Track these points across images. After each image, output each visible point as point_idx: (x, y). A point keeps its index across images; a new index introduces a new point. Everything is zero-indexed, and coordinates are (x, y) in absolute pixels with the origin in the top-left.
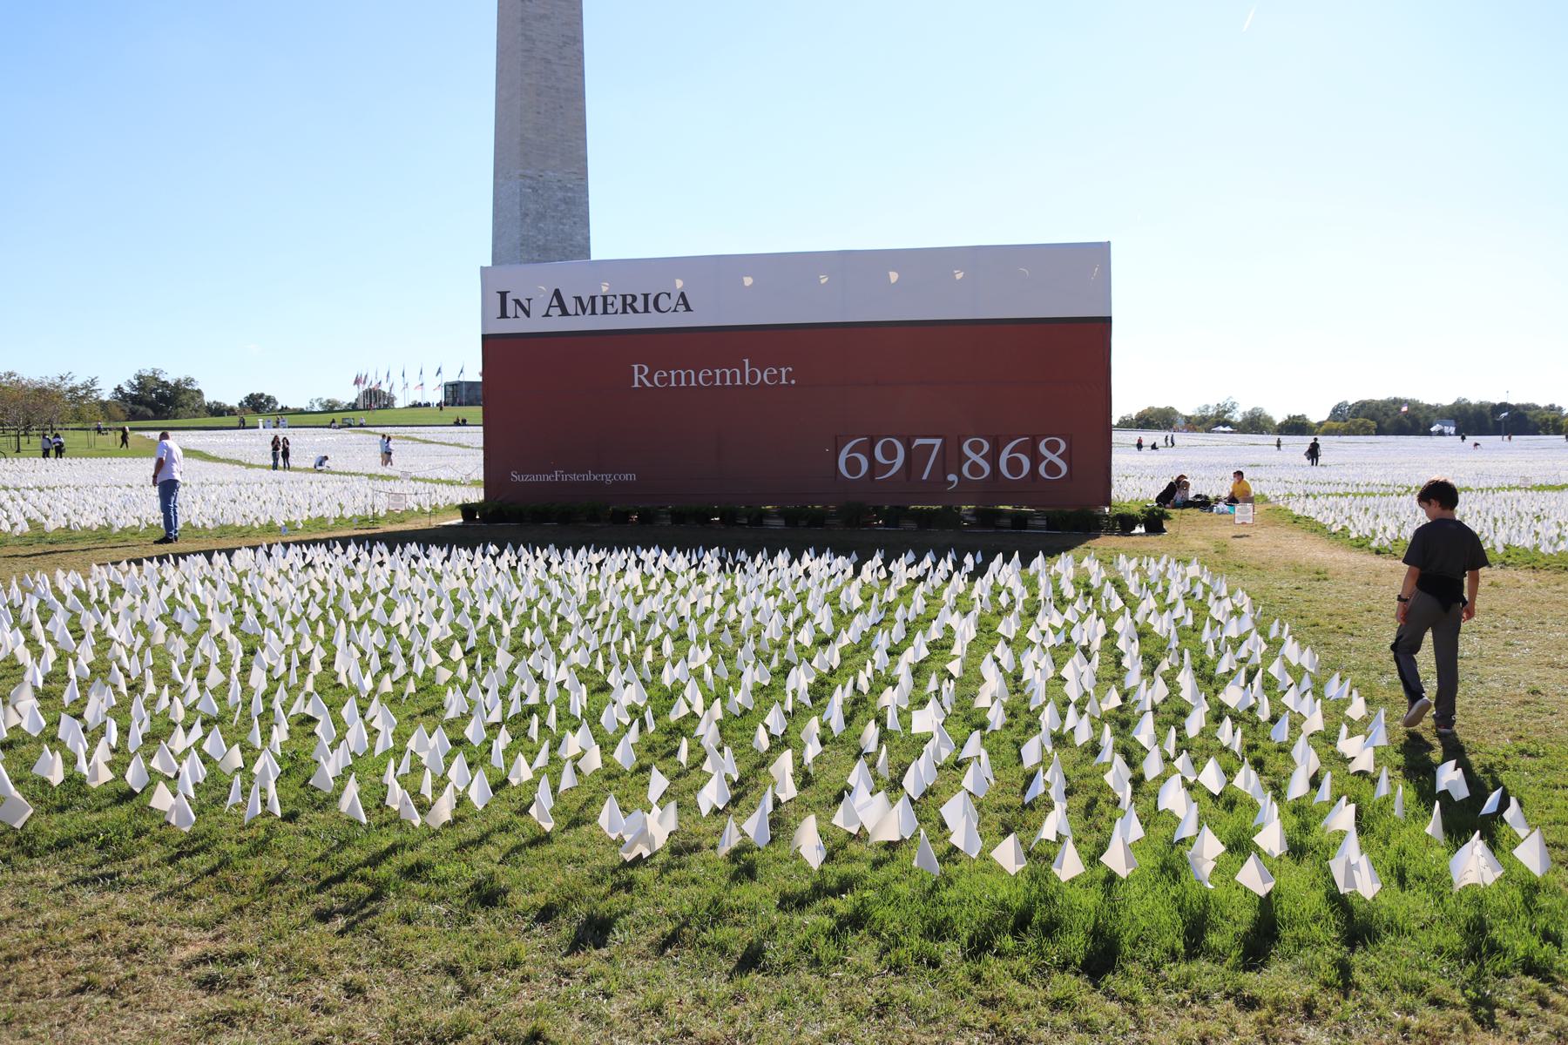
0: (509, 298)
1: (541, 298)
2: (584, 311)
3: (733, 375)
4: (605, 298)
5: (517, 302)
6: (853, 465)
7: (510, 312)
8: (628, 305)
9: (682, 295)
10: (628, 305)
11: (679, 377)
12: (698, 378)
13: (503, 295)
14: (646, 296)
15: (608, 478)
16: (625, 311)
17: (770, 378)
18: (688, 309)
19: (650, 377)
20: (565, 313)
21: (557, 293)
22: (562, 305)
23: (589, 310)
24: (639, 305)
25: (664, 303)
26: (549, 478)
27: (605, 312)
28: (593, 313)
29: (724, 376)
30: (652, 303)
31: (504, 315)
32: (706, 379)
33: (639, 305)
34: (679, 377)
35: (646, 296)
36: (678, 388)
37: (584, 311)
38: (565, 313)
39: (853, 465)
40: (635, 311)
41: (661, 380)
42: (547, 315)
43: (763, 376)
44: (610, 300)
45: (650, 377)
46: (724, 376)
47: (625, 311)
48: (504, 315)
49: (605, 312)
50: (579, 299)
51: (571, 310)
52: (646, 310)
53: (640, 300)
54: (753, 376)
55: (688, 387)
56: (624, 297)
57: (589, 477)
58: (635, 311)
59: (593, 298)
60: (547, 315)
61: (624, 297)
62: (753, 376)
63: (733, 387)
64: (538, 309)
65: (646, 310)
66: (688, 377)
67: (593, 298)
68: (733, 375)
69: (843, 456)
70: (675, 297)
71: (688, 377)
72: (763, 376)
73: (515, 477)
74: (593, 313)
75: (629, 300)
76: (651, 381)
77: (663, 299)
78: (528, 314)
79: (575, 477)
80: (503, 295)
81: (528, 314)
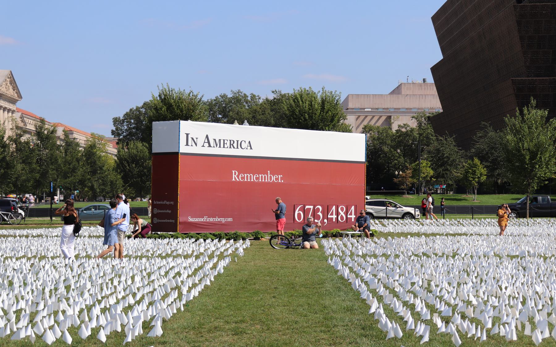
0: (190, 136)
2: (217, 145)
3: (265, 177)
4: (224, 140)
5: (192, 139)
6: (299, 215)
7: (190, 143)
9: (249, 142)
10: (231, 145)
13: (187, 135)
14: (238, 141)
15: (223, 220)
16: (230, 147)
17: (277, 179)
18: (251, 148)
19: (238, 176)
20: (210, 146)
21: (207, 137)
22: (209, 142)
23: (218, 146)
24: (235, 145)
26: (202, 220)
27: (224, 147)
28: (220, 147)
30: (240, 145)
31: (187, 145)
32: (257, 178)
33: (235, 145)
35: (238, 141)
36: (247, 182)
37: (217, 145)
38: (210, 146)
39: (299, 215)
40: (234, 148)
41: (242, 178)
42: (203, 146)
43: (274, 178)
44: (226, 142)
45: (238, 176)
47: (230, 147)
48: (187, 145)
49: (224, 147)
50: (215, 140)
51: (212, 145)
52: (237, 148)
53: (236, 142)
54: (271, 177)
55: (251, 182)
56: (230, 141)
57: (217, 219)
58: (234, 148)
59: (220, 140)
60: (203, 146)
61: (230, 141)
62: (271, 179)
63: (265, 183)
64: (200, 142)
65: (237, 148)
66: (251, 176)
67: (220, 140)
68: (265, 177)
70: (247, 142)
71: (251, 176)
72: (274, 178)
73: (191, 220)
74: (220, 147)
75: (232, 143)
76: (239, 179)
77: (243, 142)
78: (196, 144)
79: (211, 220)
80: (187, 135)
81: (196, 144)
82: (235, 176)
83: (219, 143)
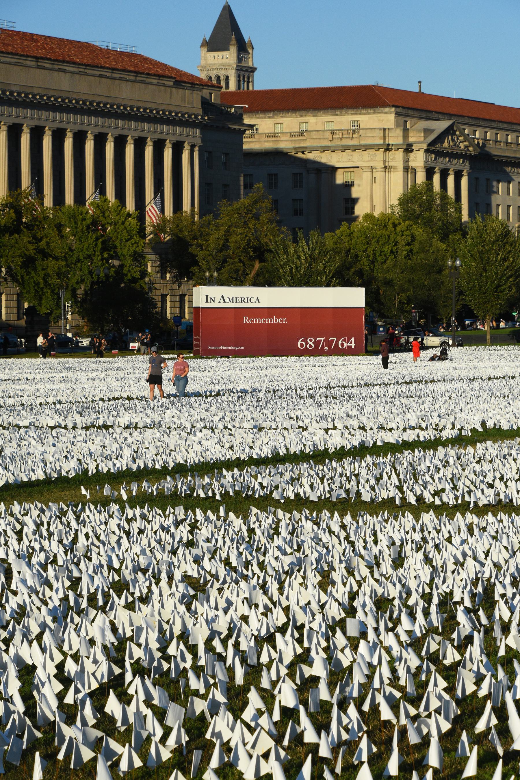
1: (218, 298)
6: (302, 345)
8: (242, 300)
10: (242, 300)
11: (257, 321)
12: (262, 321)
25: (252, 300)
29: (268, 321)
30: (249, 300)
34: (257, 321)
39: (302, 345)
43: (279, 321)
46: (268, 321)
64: (217, 300)
69: (299, 343)
72: (279, 321)
82: (246, 320)
83: (231, 300)
